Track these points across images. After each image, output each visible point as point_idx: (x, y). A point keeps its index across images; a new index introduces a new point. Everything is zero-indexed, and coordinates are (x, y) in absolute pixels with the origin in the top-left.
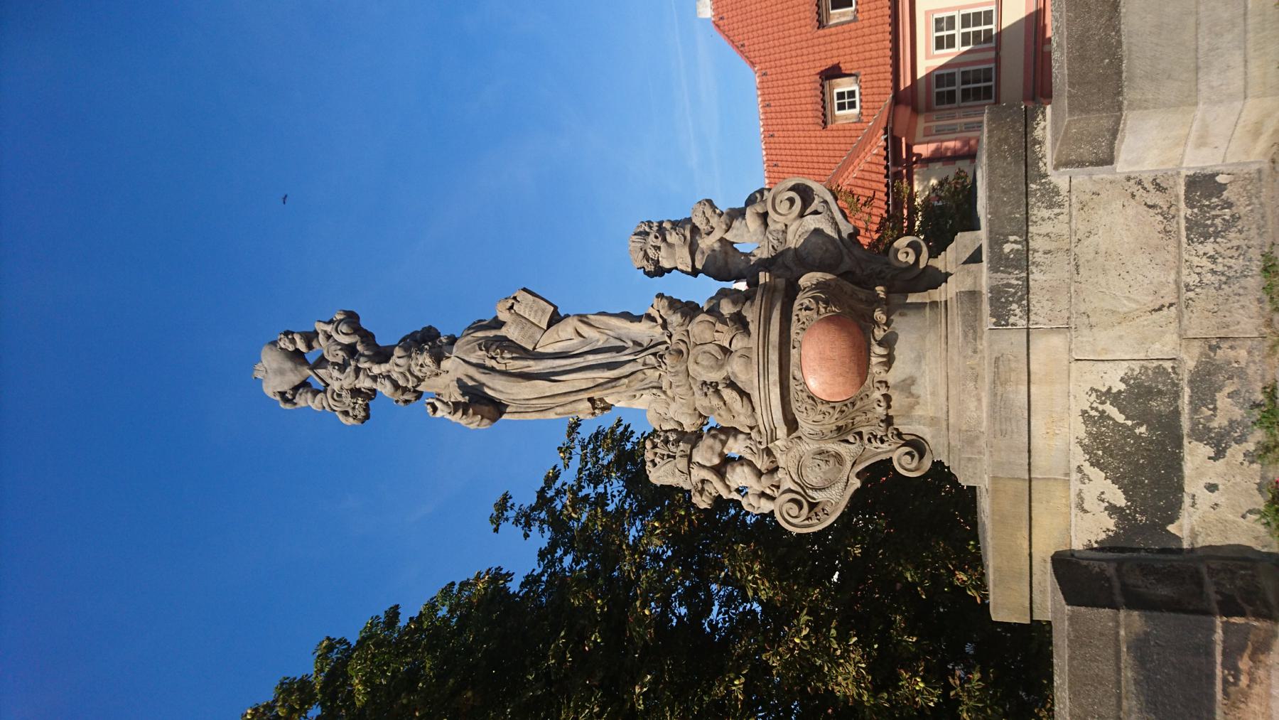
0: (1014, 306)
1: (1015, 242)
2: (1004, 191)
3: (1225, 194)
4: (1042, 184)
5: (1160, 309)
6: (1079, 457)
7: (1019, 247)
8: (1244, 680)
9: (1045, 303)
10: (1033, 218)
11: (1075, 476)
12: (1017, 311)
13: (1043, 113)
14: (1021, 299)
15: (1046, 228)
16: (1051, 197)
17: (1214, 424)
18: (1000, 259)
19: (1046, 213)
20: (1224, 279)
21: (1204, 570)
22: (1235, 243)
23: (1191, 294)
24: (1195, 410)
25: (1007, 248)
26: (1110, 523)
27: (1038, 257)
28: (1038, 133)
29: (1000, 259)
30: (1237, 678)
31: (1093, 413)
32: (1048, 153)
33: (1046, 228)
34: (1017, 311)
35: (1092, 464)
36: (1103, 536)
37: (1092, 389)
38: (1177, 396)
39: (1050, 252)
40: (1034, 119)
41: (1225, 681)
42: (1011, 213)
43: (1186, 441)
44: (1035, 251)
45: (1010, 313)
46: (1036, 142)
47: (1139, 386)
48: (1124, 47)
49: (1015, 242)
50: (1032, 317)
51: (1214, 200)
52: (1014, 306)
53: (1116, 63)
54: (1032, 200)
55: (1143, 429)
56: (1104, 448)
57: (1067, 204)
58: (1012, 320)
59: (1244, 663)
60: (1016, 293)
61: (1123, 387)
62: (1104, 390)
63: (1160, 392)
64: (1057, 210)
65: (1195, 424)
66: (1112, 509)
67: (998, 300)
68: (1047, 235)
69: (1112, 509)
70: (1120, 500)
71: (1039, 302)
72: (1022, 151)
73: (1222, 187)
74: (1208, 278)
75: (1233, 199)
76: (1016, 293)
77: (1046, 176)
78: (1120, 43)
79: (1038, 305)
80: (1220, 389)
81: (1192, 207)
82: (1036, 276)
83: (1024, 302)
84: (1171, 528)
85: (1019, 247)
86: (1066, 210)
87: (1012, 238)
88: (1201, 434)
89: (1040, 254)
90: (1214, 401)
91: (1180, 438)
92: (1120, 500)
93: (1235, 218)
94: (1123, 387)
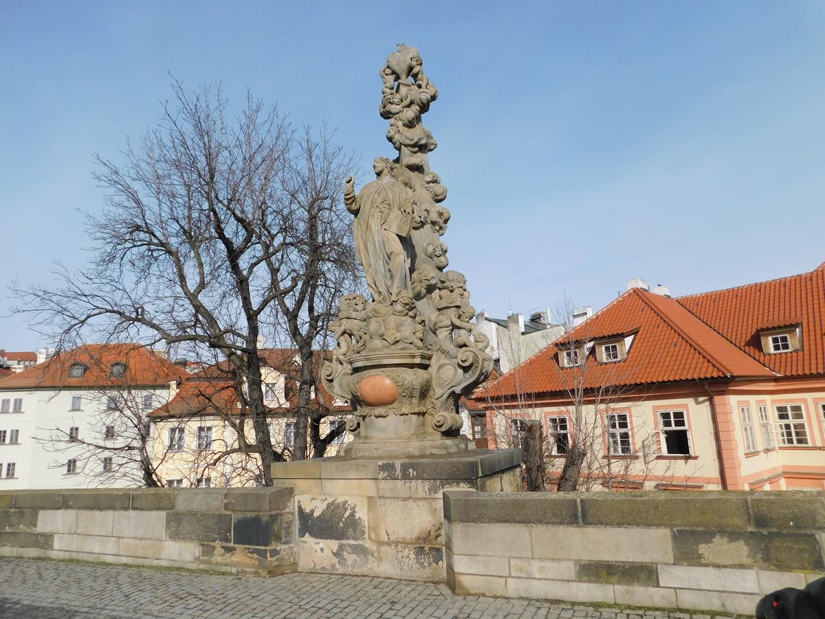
0: (387, 473)
1: (413, 474)
2: (436, 469)
3: (434, 564)
4: (439, 487)
5: (388, 535)
6: (330, 500)
8: (250, 555)
11: (323, 497)
12: (385, 475)
13: (471, 487)
15: (420, 488)
16: (433, 490)
17: (345, 553)
19: (426, 488)
20: (400, 561)
21: (292, 545)
22: (414, 566)
23: (394, 547)
24: (350, 546)
25: (411, 470)
26: (307, 511)
27: (408, 484)
28: (462, 485)
30: (250, 553)
31: (347, 505)
32: (452, 489)
33: (420, 488)
34: (385, 475)
35: (328, 504)
36: (303, 508)
37: (356, 505)
38: (354, 539)
40: (468, 483)
41: (250, 549)
43: (338, 541)
45: (384, 471)
46: (458, 483)
47: (358, 524)
48: (482, 524)
49: (413, 474)
51: (432, 559)
52: (387, 473)
53: (475, 521)
54: (432, 481)
55: (342, 525)
56: (334, 510)
57: (430, 497)
58: (381, 473)
59: (255, 556)
61: (357, 517)
62: (356, 510)
63: (355, 532)
64: (428, 492)
65: (345, 545)
66: (312, 511)
67: (389, 467)
69: (312, 511)
70: (316, 514)
72: (453, 477)
73: (437, 563)
74: (400, 554)
75: (432, 567)
77: (443, 488)
78: (484, 522)
80: (358, 556)
81: (429, 550)
82: (399, 483)
84: (307, 534)
86: (428, 496)
87: (415, 472)
88: (341, 547)
90: (353, 553)
91: (339, 539)
92: (316, 514)
93: (424, 567)
94: (357, 517)
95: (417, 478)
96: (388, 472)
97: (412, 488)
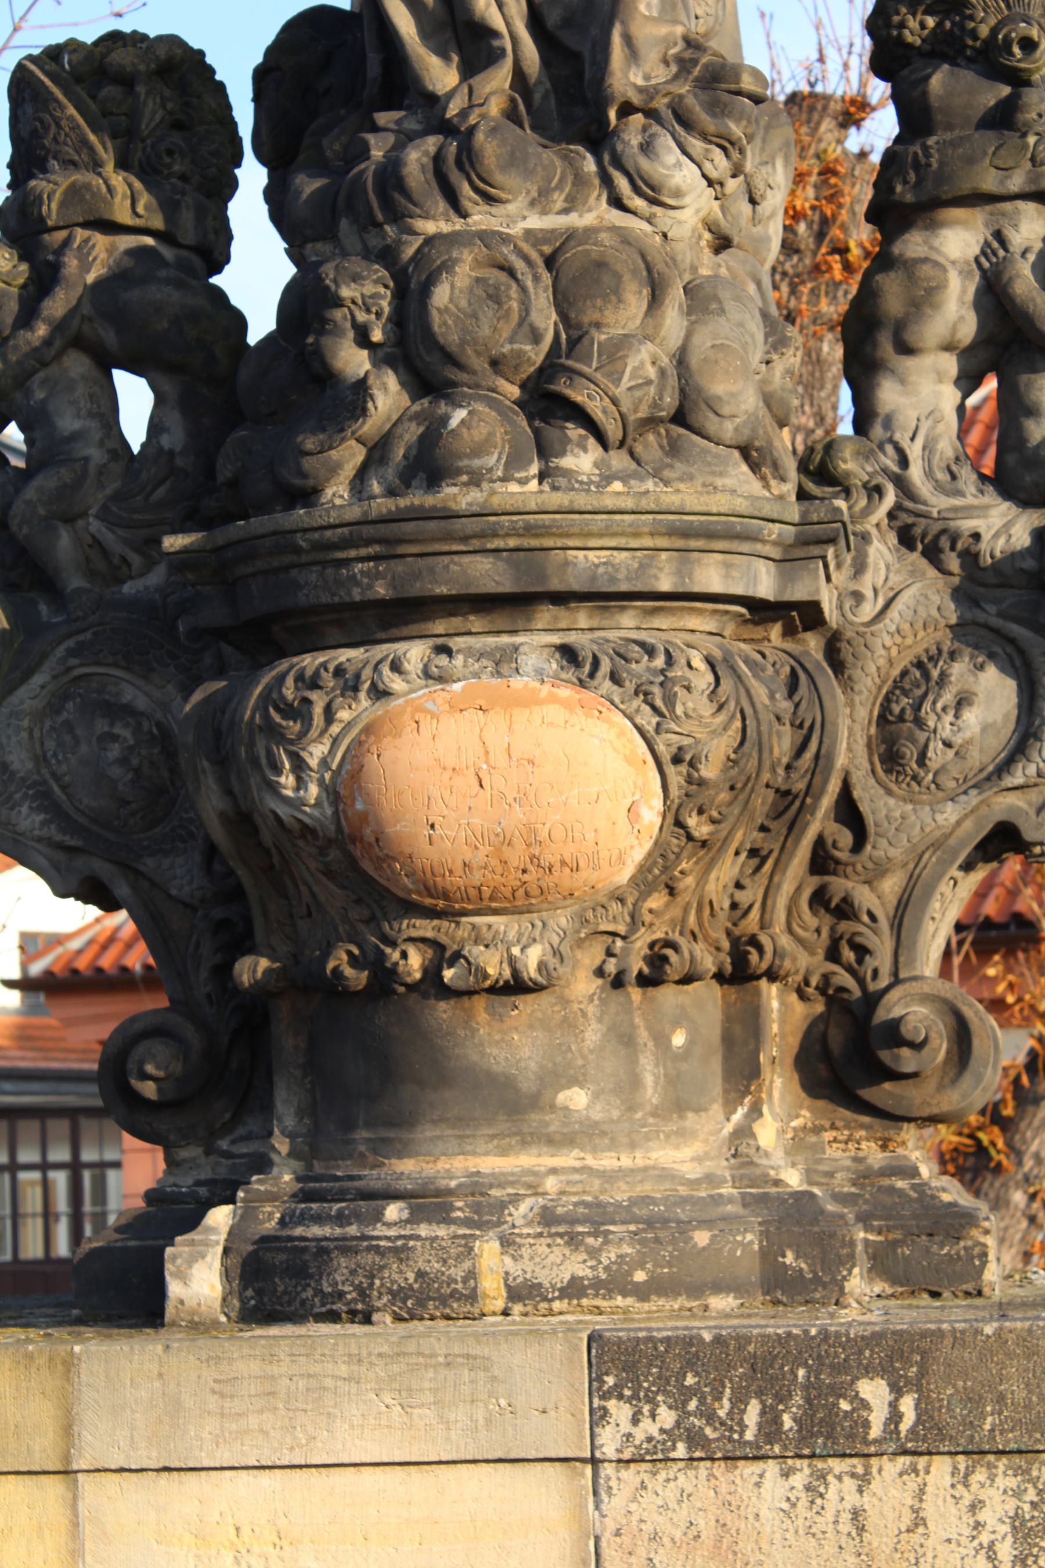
0: (667, 1417)
1: (895, 1416)
7: (876, 1431)
9: (683, 1513)
10: (980, 1476)
12: (648, 1427)
14: (694, 1439)
15: (946, 1517)
18: (837, 1369)
19: (997, 1512)
25: (874, 1391)
29: (837, 1369)
33: (946, 1517)
34: (648, 1427)
39: (861, 1529)
42: (1001, 1398)
44: (864, 1480)
49: (895, 1416)
50: (631, 1475)
52: (667, 1417)
58: (620, 1411)
60: (710, 1417)
67: (690, 1364)
68: (919, 1521)
71: (684, 1496)
76: (710, 1417)
79: (670, 1493)
82: (768, 1489)
83: (681, 1450)
85: (876, 1431)
87: (907, 1405)
89: (852, 1499)
95: (919, 1445)
96: (679, 1406)
97: (872, 1521)
